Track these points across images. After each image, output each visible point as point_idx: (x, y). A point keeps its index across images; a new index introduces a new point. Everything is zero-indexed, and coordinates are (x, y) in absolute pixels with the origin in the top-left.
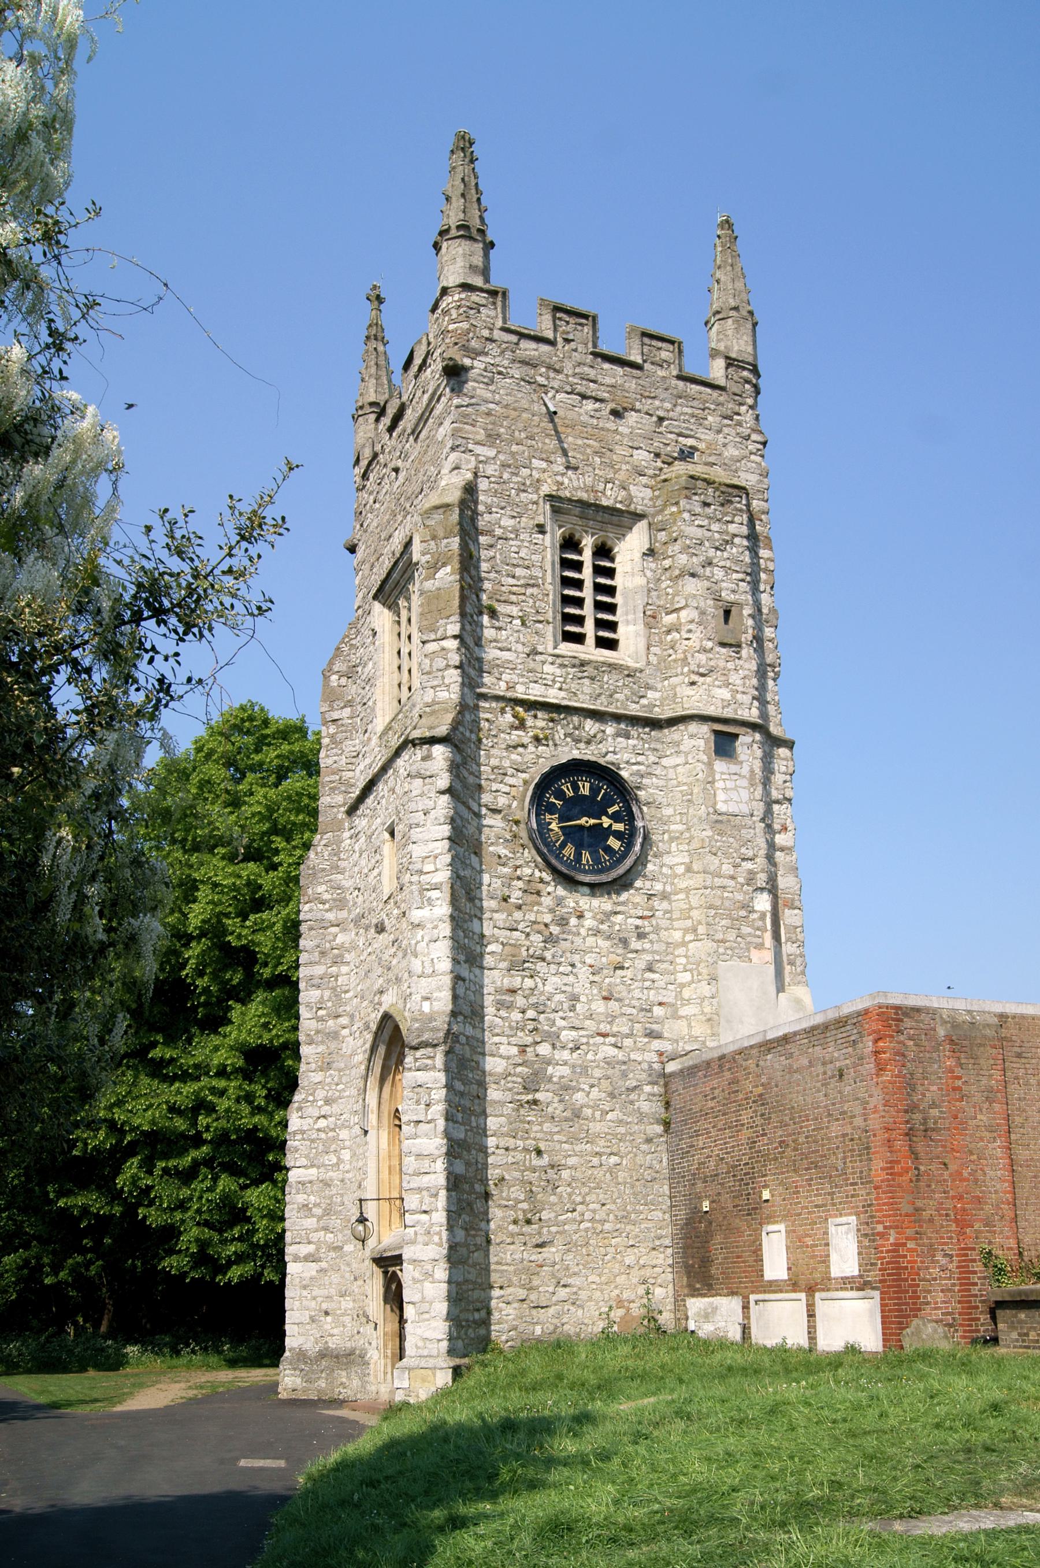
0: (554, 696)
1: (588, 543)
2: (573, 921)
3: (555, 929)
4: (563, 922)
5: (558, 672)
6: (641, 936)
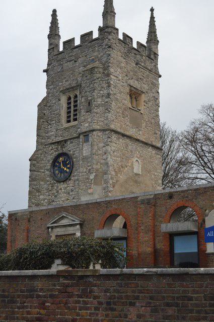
0: (60, 139)
1: (72, 96)
2: (60, 191)
3: (56, 194)
4: (57, 192)
5: (62, 132)
6: (72, 191)
